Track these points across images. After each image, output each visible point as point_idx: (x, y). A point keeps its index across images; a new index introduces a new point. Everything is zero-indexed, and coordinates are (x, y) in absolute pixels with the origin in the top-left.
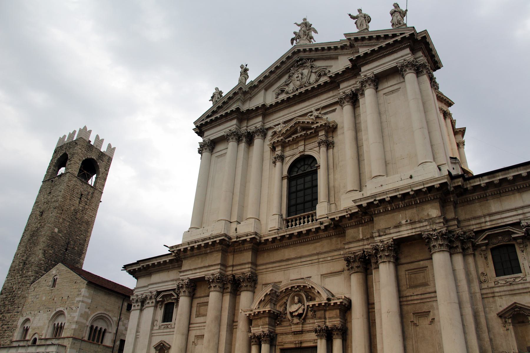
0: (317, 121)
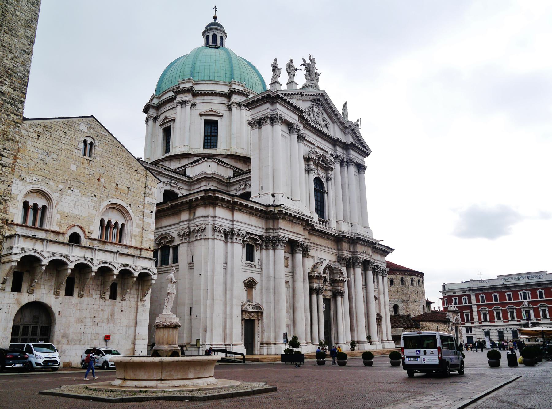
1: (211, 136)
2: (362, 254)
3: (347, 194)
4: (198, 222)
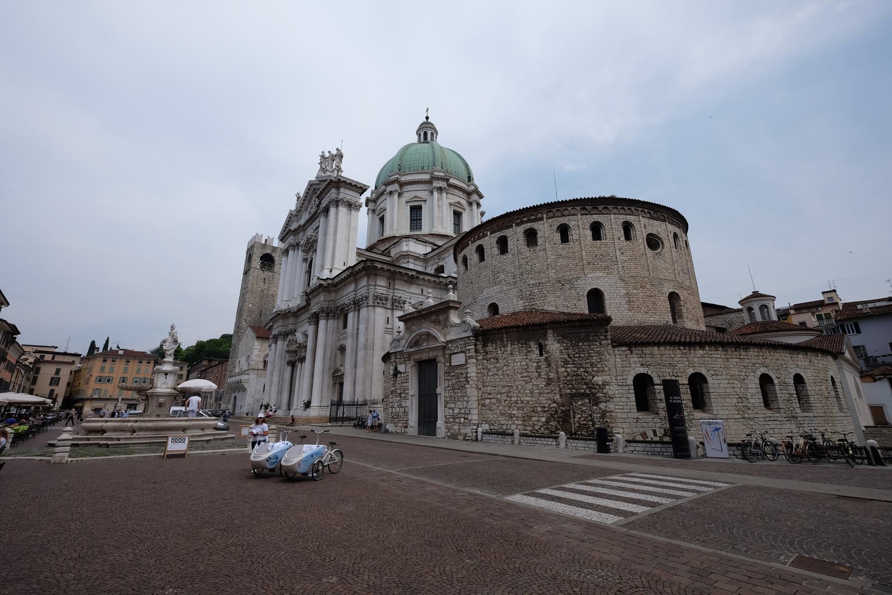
1: (417, 220)
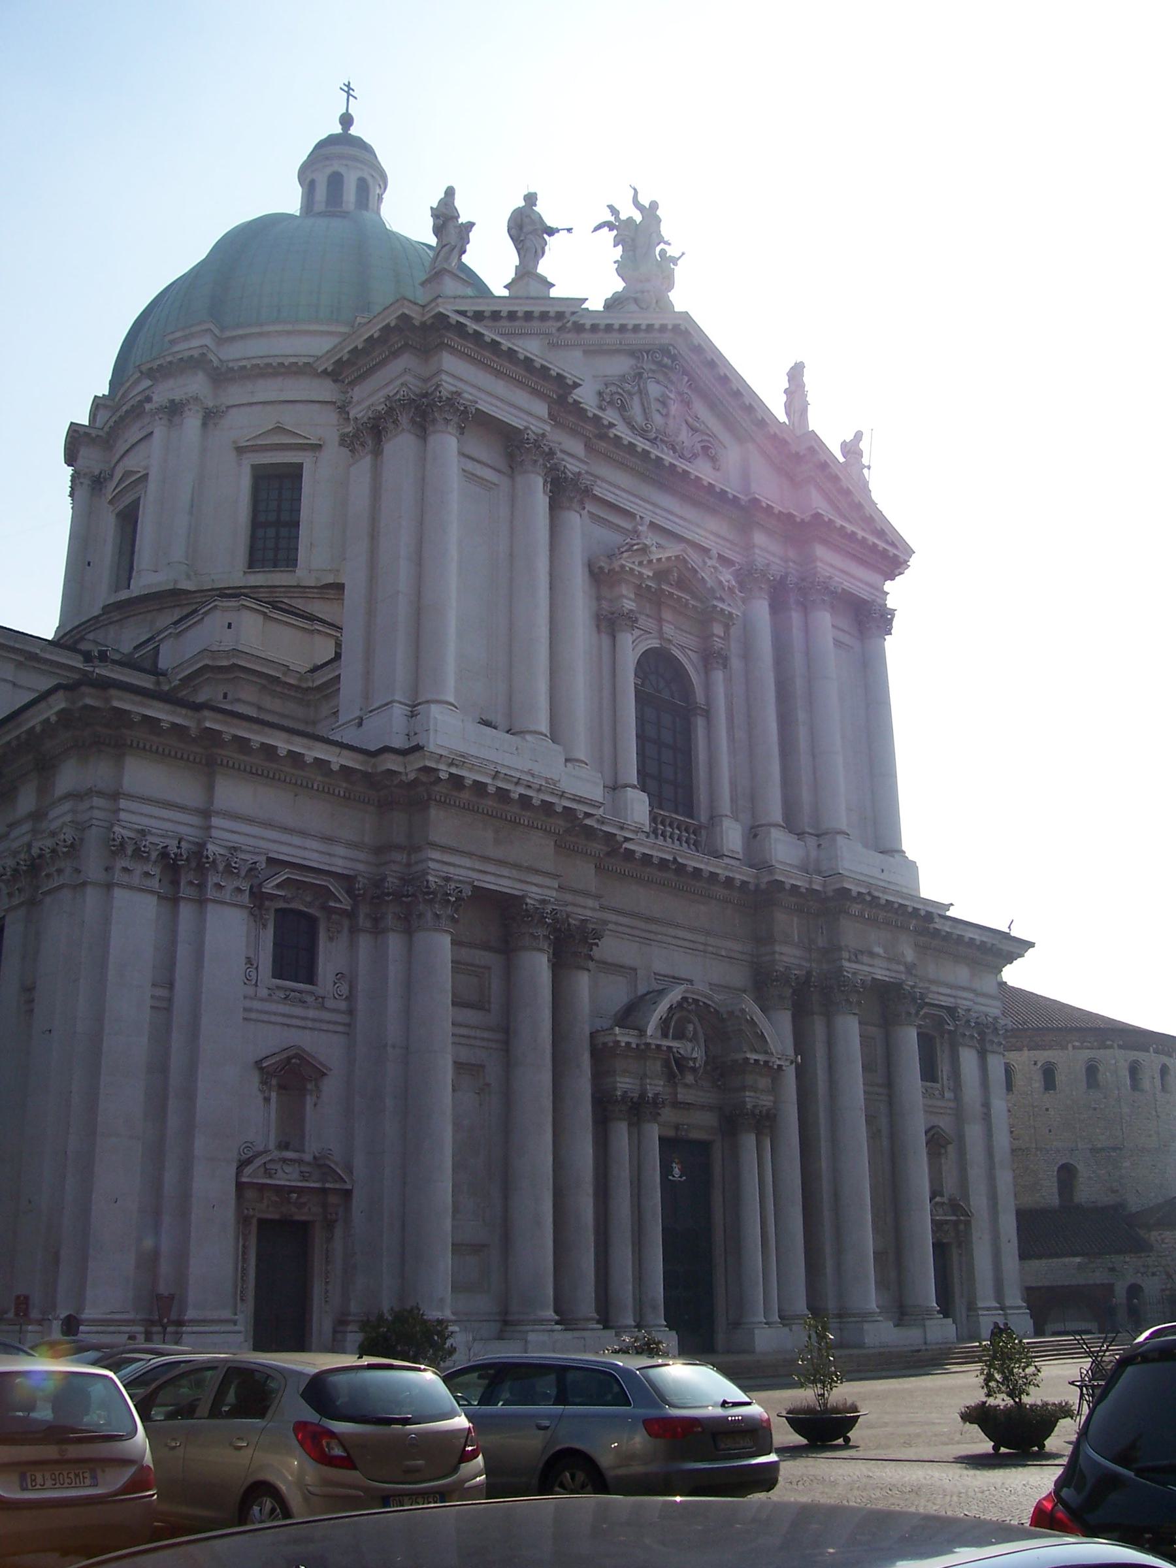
0: (724, 597)
2: (865, 959)
3: (801, 716)
4: (61, 816)
